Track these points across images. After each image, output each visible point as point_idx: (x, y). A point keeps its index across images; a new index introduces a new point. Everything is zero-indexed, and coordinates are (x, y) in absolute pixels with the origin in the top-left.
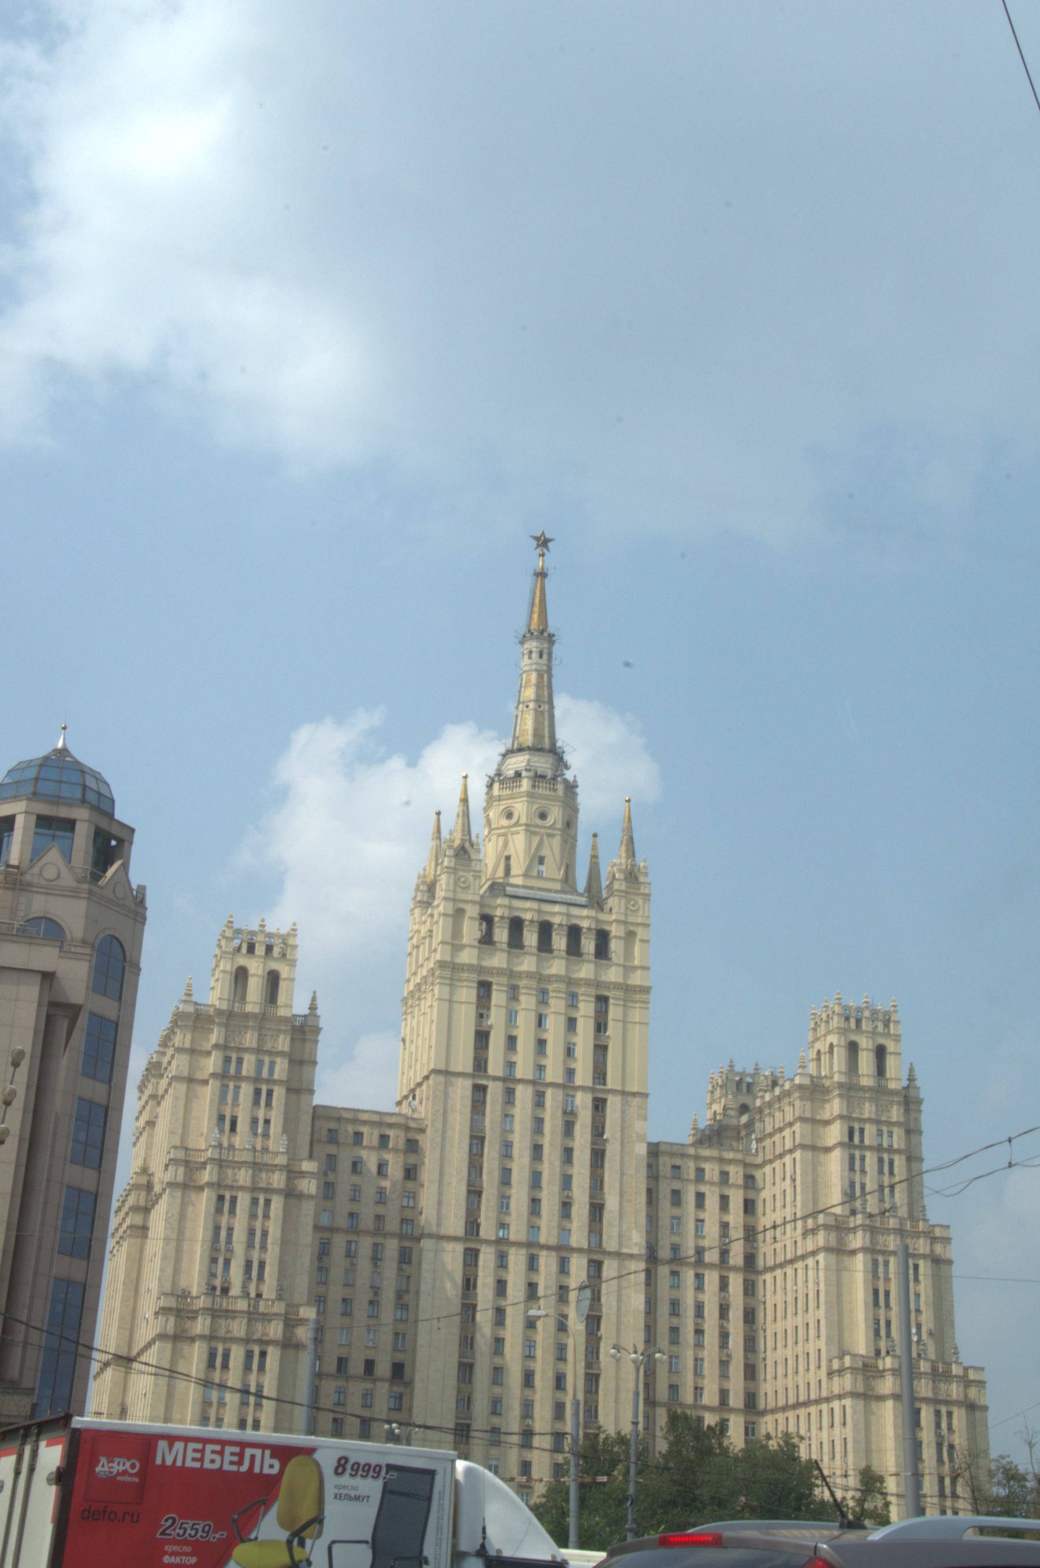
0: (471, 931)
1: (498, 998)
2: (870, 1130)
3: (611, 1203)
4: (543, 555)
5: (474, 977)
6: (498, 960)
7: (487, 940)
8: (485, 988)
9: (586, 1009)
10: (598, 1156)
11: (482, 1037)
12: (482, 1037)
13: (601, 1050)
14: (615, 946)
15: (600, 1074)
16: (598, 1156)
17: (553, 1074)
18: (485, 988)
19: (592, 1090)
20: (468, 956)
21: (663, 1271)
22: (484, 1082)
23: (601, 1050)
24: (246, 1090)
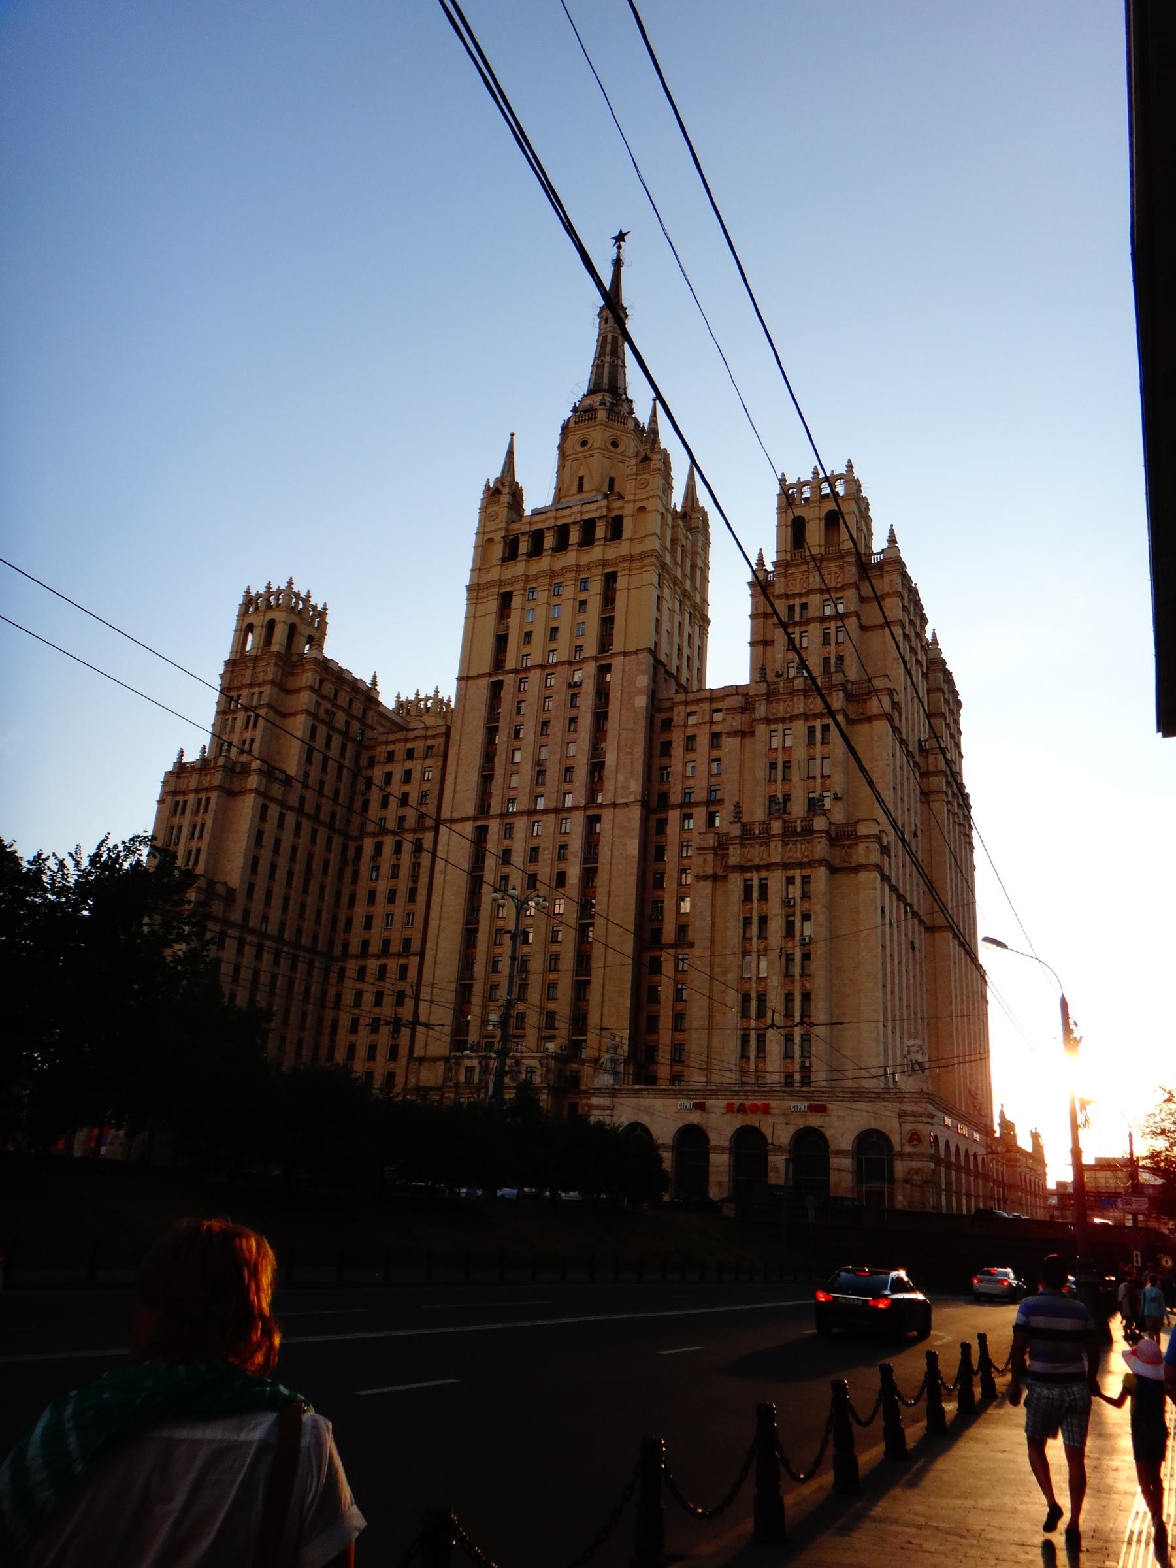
0: (498, 551)
1: (516, 602)
2: (815, 600)
3: (610, 759)
4: (619, 247)
5: (495, 590)
6: (519, 568)
7: (511, 553)
8: (506, 600)
9: (596, 587)
10: (600, 717)
11: (501, 641)
12: (501, 641)
13: (607, 623)
14: (627, 524)
15: (605, 643)
16: (600, 717)
17: (563, 653)
18: (506, 600)
19: (596, 659)
20: (495, 574)
21: (674, 816)
22: (501, 678)
23: (607, 623)
24: (241, 716)
